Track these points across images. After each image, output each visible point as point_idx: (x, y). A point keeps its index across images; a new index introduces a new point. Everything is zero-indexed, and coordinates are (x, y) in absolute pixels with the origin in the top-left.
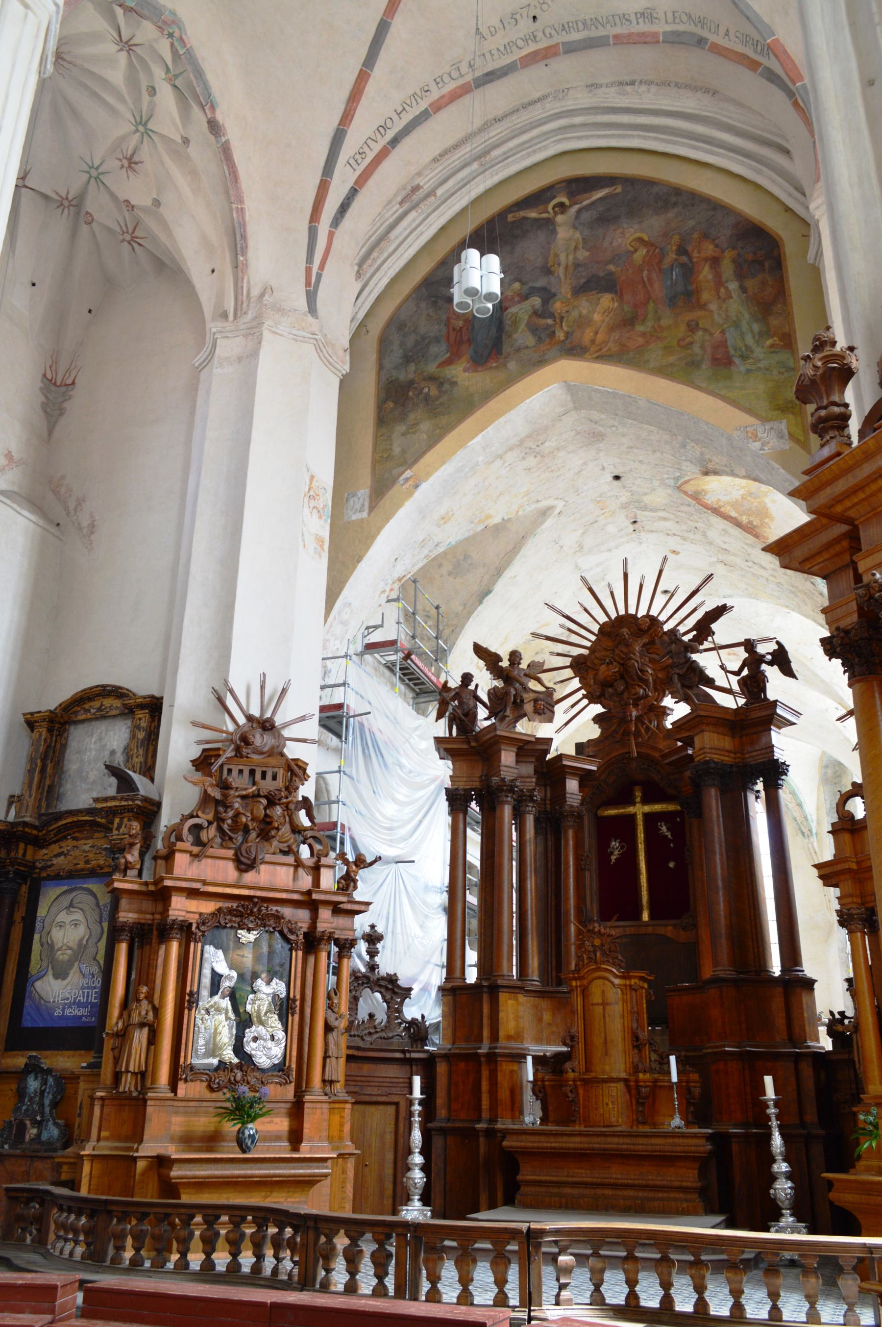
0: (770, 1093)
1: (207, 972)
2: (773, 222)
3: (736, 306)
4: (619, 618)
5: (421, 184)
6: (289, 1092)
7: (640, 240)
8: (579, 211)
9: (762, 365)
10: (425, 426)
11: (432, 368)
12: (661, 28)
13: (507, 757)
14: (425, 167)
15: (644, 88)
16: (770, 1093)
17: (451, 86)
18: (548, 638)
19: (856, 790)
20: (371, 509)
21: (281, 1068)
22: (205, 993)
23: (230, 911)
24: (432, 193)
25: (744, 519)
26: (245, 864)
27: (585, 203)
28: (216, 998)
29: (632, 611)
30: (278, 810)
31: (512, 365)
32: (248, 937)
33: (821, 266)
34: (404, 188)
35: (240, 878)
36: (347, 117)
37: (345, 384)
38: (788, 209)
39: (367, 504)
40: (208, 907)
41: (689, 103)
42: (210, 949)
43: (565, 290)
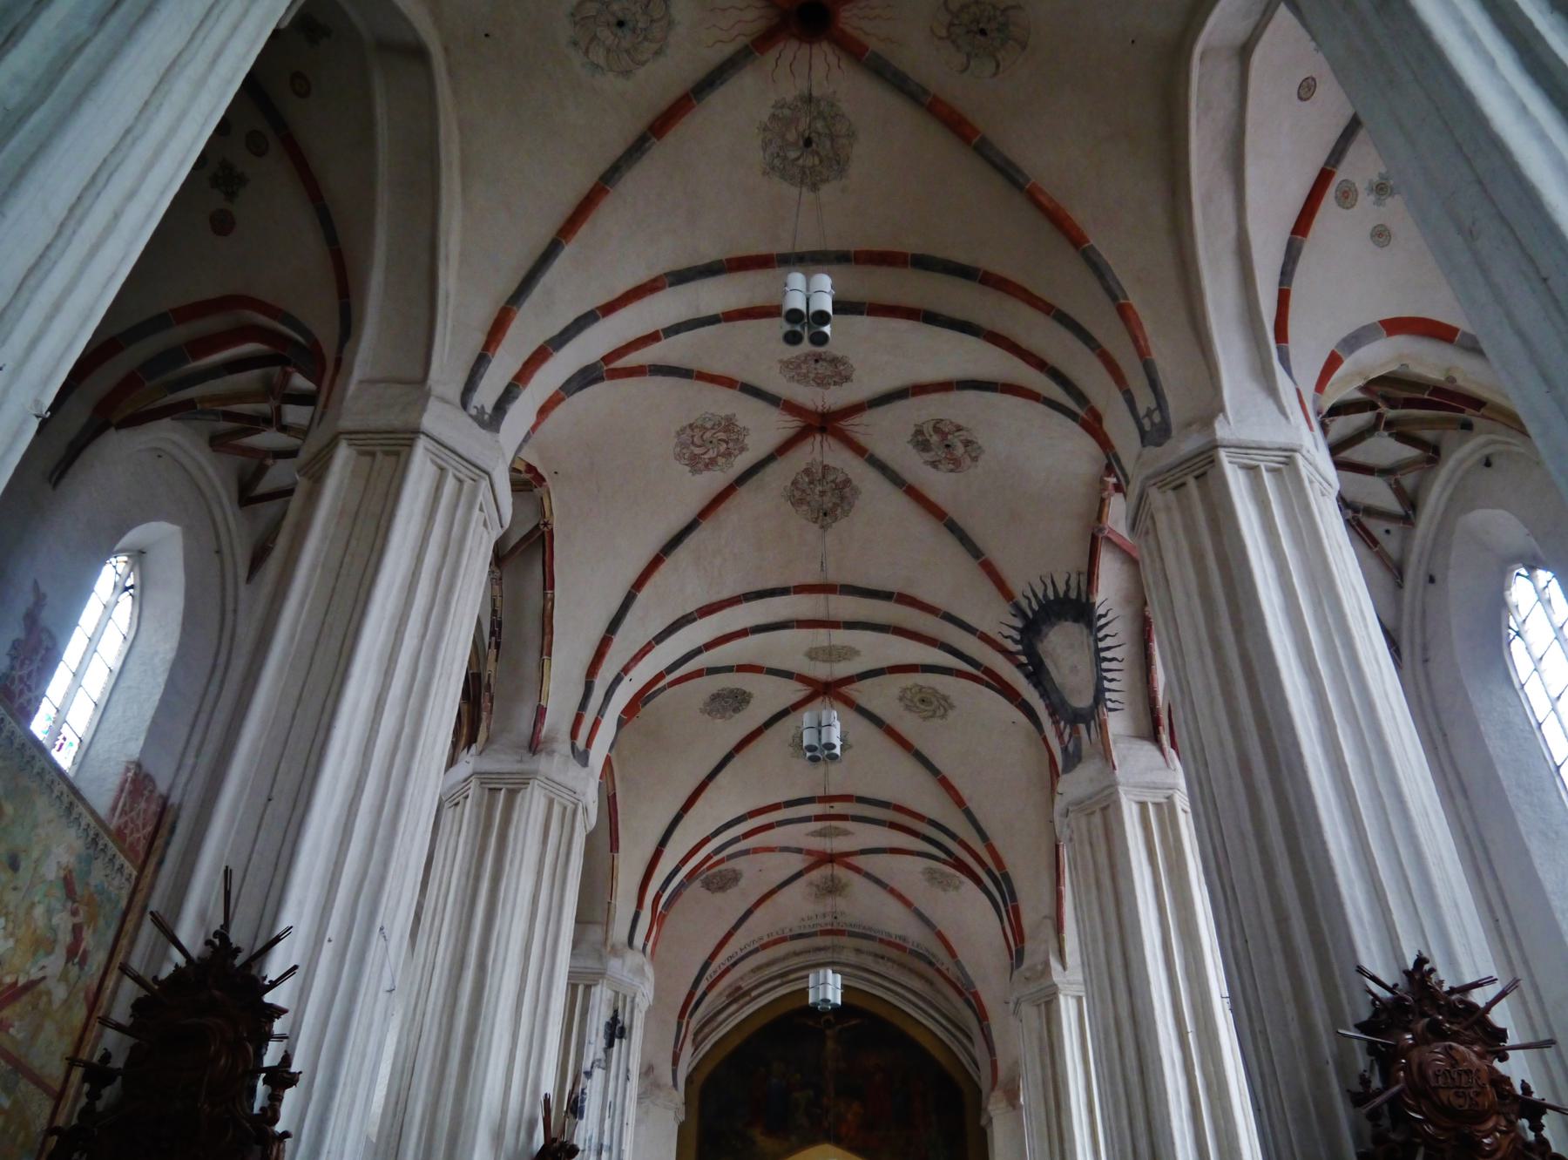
5: (743, 986)
12: (909, 946)
14: (745, 975)
15: (890, 964)
17: (776, 937)
27: (846, 1025)
33: (988, 1131)
34: (730, 986)
37: (682, 1129)
38: (967, 1071)
41: (916, 984)
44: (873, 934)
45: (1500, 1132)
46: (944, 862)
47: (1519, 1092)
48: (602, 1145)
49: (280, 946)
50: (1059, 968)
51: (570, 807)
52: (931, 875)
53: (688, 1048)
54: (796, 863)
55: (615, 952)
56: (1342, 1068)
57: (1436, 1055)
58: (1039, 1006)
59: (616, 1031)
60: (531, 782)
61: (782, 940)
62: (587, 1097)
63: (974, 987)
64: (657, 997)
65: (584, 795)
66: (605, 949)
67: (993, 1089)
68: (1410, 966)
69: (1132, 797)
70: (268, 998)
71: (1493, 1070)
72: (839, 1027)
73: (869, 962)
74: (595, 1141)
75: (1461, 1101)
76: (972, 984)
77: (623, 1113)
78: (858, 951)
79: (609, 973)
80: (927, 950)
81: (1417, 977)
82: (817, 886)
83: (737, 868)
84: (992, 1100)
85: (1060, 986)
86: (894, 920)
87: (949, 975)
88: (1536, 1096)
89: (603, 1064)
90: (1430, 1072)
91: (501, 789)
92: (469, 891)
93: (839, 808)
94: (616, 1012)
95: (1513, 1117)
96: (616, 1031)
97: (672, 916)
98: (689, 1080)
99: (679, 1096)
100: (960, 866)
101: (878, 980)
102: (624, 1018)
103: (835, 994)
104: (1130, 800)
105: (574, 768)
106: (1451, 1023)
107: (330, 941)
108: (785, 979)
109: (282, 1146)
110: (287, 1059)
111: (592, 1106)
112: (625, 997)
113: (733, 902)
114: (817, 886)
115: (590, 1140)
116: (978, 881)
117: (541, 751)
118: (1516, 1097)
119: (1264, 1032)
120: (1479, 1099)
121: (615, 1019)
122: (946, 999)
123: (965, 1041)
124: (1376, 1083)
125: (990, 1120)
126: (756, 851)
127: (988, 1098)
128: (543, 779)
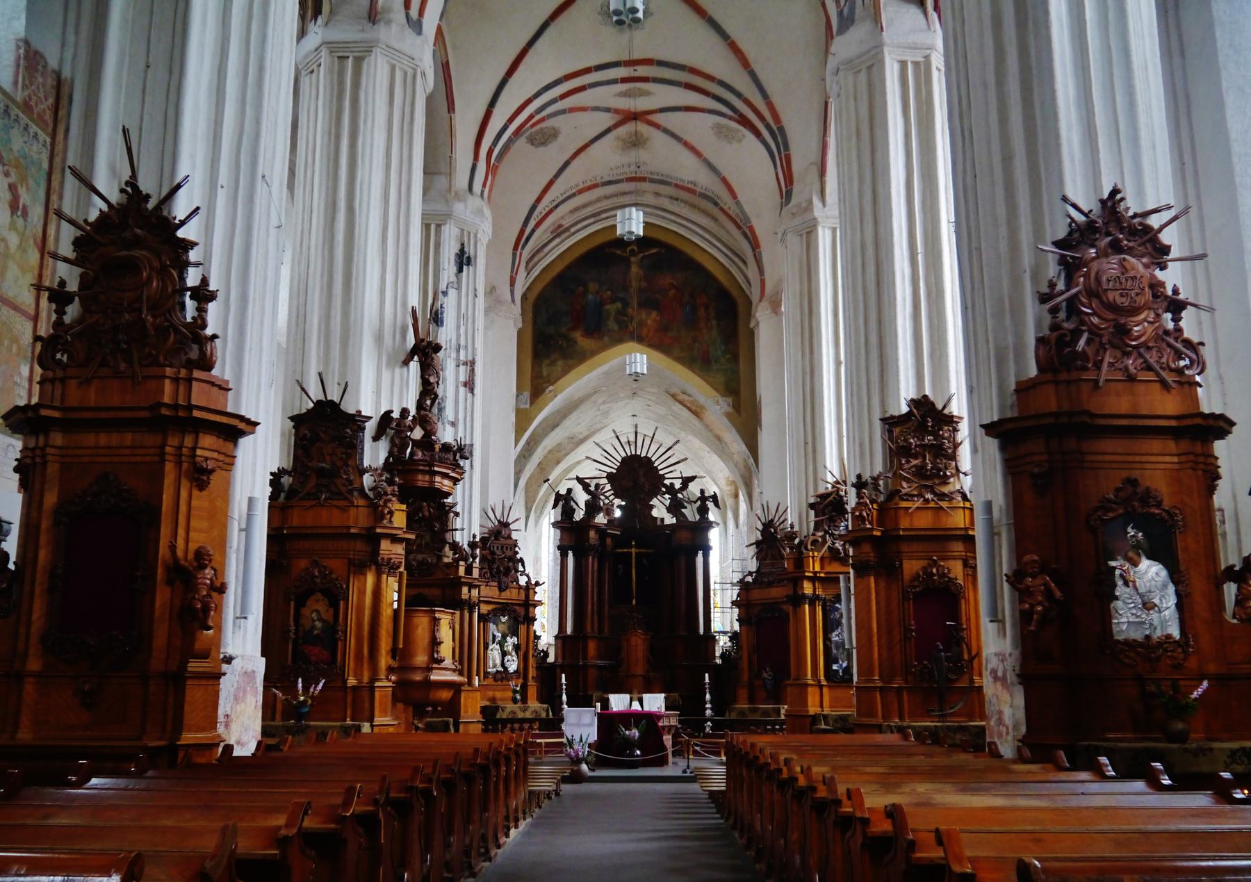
0: (707, 680)
1: (491, 635)
2: (735, 293)
3: (715, 333)
4: (632, 455)
6: (521, 681)
7: (672, 284)
8: (643, 258)
9: (724, 367)
10: (560, 363)
11: (564, 330)
12: (699, 190)
13: (592, 534)
15: (682, 205)
16: (707, 680)
17: (589, 183)
18: (595, 461)
19: (750, 574)
20: (531, 404)
21: (515, 672)
22: (491, 643)
23: (500, 609)
24: (568, 229)
25: (694, 408)
26: (501, 590)
27: (647, 253)
28: (495, 644)
29: (638, 453)
30: (511, 564)
31: (606, 339)
32: (504, 619)
33: (756, 331)
34: (554, 224)
35: (500, 595)
36: (539, 200)
37: (520, 334)
38: (741, 287)
39: (529, 401)
40: (490, 607)
41: (704, 221)
42: (491, 624)
43: (635, 303)
44: (669, 180)
45: (1149, 322)
46: (731, 118)
47: (1170, 293)
48: (459, 345)
49: (181, 192)
50: (820, 205)
51: (410, 72)
52: (718, 129)
53: (522, 273)
54: (606, 120)
55: (458, 197)
56: (1035, 277)
57: (1111, 266)
58: (801, 235)
59: (463, 260)
60: (374, 49)
61: (595, 186)
62: (445, 310)
63: (750, 222)
64: (494, 233)
65: (421, 60)
66: (449, 194)
67: (761, 300)
68: (1106, 195)
69: (894, 56)
70: (181, 233)
71: (1153, 276)
72: (642, 255)
73: (666, 203)
74: (454, 342)
75: (1124, 300)
76: (747, 219)
77: (474, 321)
78: (657, 194)
79: (455, 214)
80: (713, 193)
81: (1109, 204)
82: (624, 140)
83: (556, 126)
84: (759, 308)
85: (819, 220)
86: (687, 169)
87: (731, 213)
88: (1181, 297)
89: (455, 286)
90: (1104, 279)
91: (348, 57)
92: (332, 147)
93: (642, 71)
94: (463, 245)
95: (1160, 311)
96: (463, 260)
97: (504, 168)
98: (524, 297)
99: (517, 308)
100: (744, 121)
101: (672, 217)
102: (470, 250)
103: (638, 228)
104: (892, 59)
105: (409, 34)
106: (1129, 241)
107: (222, 187)
108: (598, 218)
109: (213, 344)
110: (205, 281)
111: (449, 317)
112: (469, 233)
113: (554, 155)
114: (624, 140)
115: (450, 341)
116: (758, 134)
117: (380, 21)
118: (1167, 297)
119: (979, 249)
120: (1137, 299)
121: (462, 251)
122: (728, 232)
123: (741, 265)
124: (1061, 286)
125: (758, 323)
126: (572, 110)
127: (757, 306)
128: (384, 47)
